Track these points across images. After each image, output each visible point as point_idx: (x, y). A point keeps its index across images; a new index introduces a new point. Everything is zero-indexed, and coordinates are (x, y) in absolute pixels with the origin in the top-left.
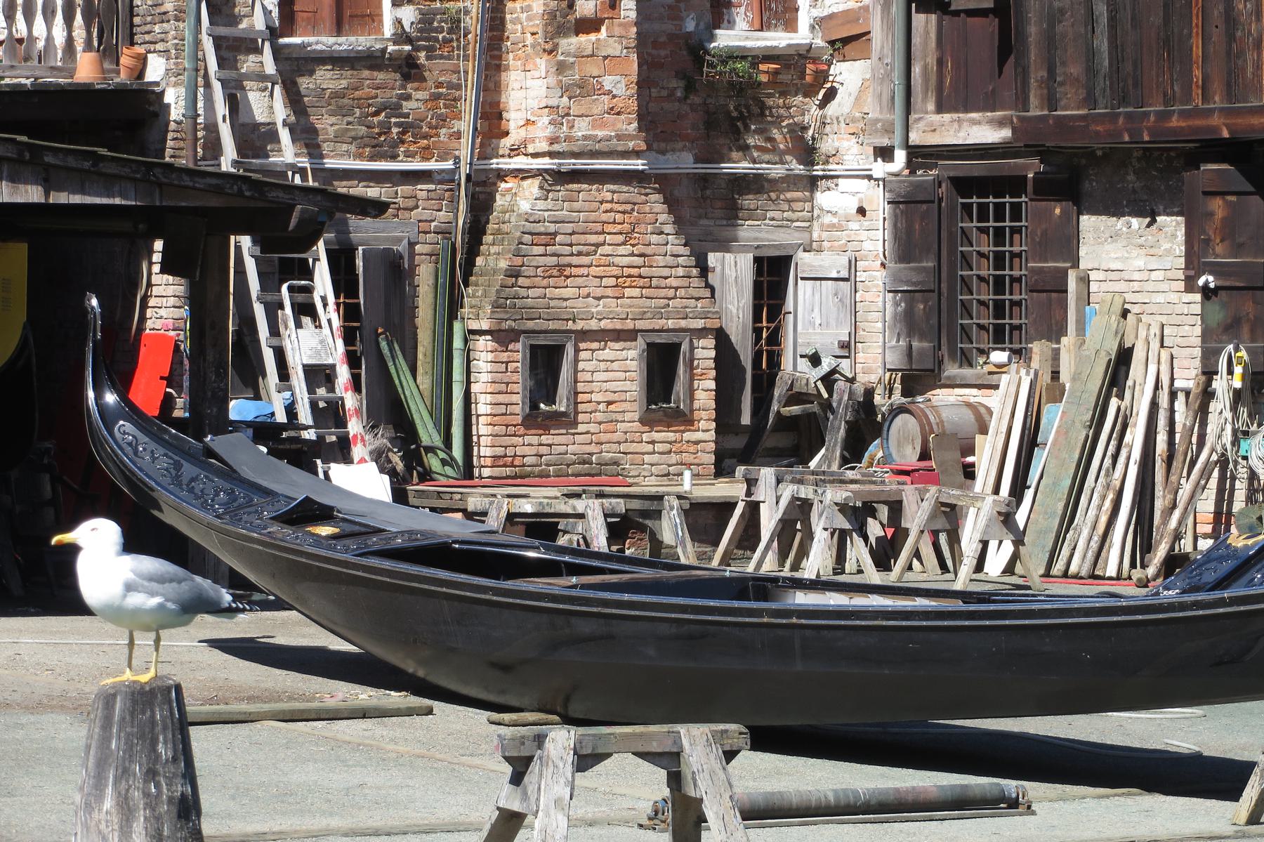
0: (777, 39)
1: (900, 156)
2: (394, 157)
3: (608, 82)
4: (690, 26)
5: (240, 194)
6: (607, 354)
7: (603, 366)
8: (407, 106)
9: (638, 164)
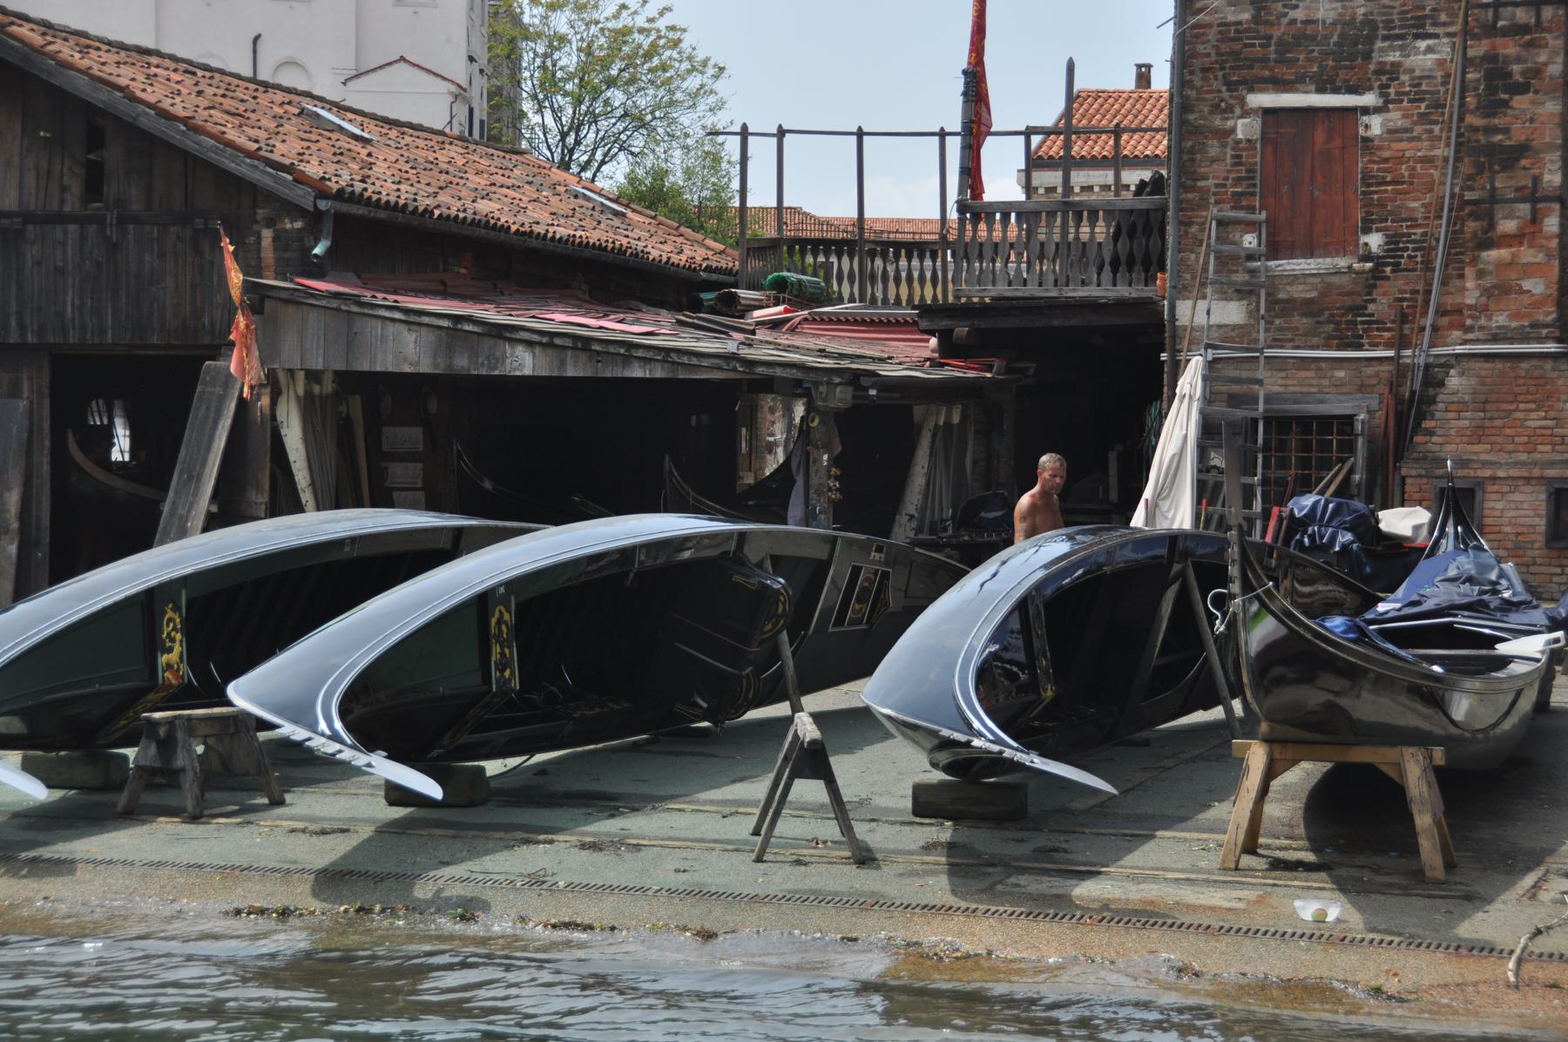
2: (1359, 347)
3: (1527, 285)
5: (735, 370)
6: (1518, 497)
7: (1513, 506)
8: (1371, 308)
9: (1552, 347)
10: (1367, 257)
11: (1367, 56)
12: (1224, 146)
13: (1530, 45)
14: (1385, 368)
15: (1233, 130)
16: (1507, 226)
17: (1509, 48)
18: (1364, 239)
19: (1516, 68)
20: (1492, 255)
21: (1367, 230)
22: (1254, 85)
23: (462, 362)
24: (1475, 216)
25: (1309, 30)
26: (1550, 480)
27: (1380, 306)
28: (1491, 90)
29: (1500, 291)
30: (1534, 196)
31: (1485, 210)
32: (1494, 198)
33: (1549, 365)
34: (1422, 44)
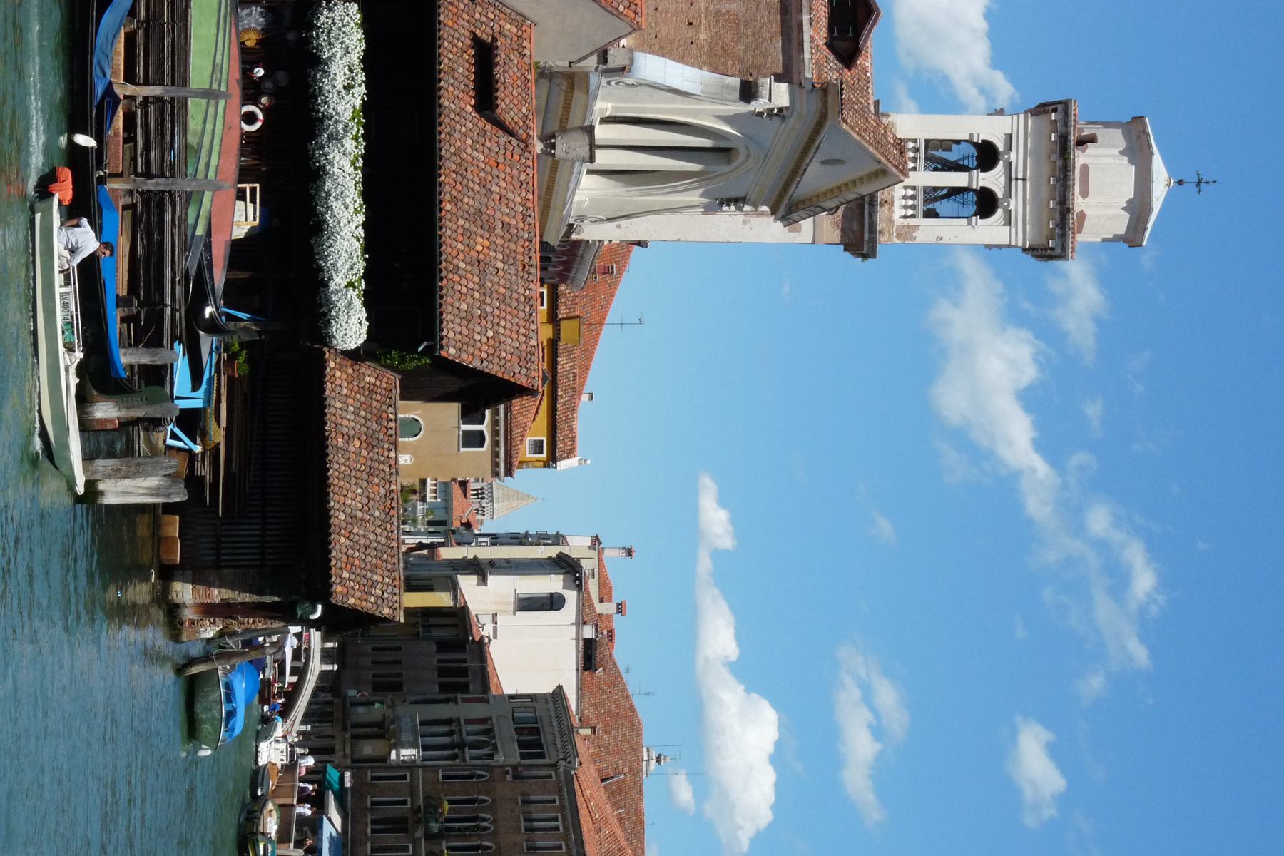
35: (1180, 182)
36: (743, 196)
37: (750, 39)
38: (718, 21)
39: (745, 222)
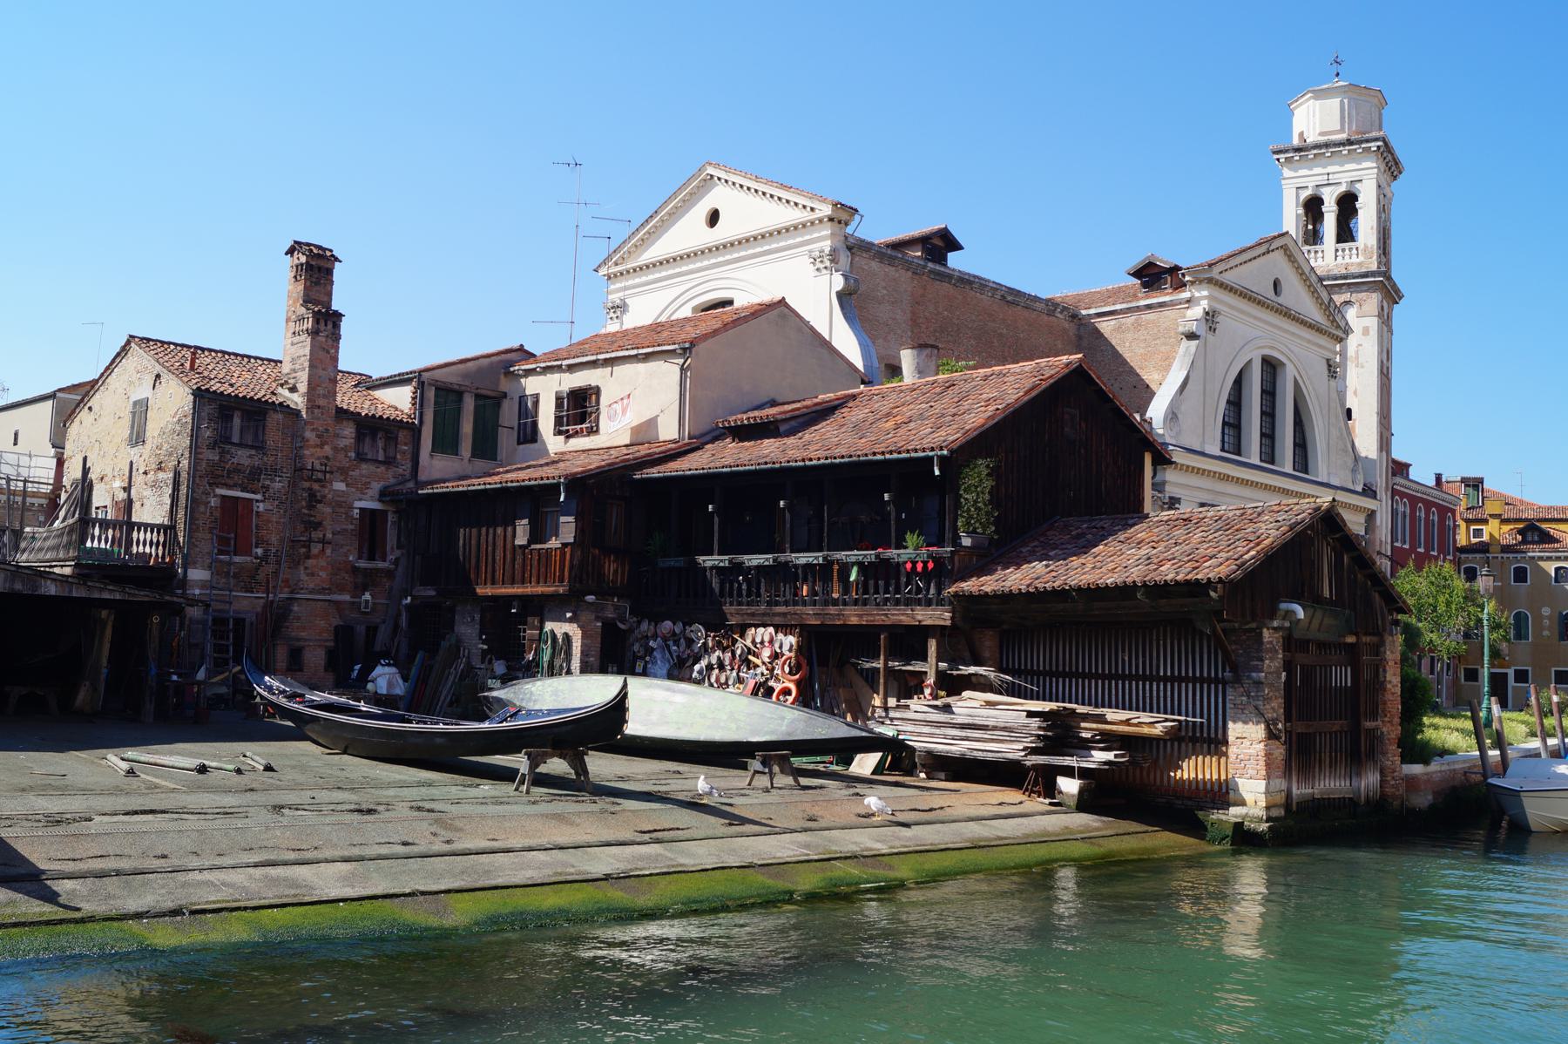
0: (380, 565)
1: (409, 598)
2: (252, 592)
4: (351, 559)
8: (257, 577)
9: (328, 597)
10: (256, 558)
11: (259, 481)
12: (206, 507)
13: (323, 486)
14: (262, 601)
15: (209, 502)
16: (315, 549)
17: (316, 486)
18: (255, 550)
19: (318, 494)
20: (310, 562)
21: (257, 547)
22: (218, 485)
23: (18, 586)
24: (304, 546)
25: (239, 467)
26: (326, 647)
27: (261, 576)
28: (310, 501)
29: (313, 574)
30: (323, 541)
31: (307, 544)
32: (310, 540)
33: (327, 603)
34: (278, 479)
35: (1338, 75)
36: (1325, 361)
37: (1158, 341)
38: (1146, 367)
39: (1362, 367)
